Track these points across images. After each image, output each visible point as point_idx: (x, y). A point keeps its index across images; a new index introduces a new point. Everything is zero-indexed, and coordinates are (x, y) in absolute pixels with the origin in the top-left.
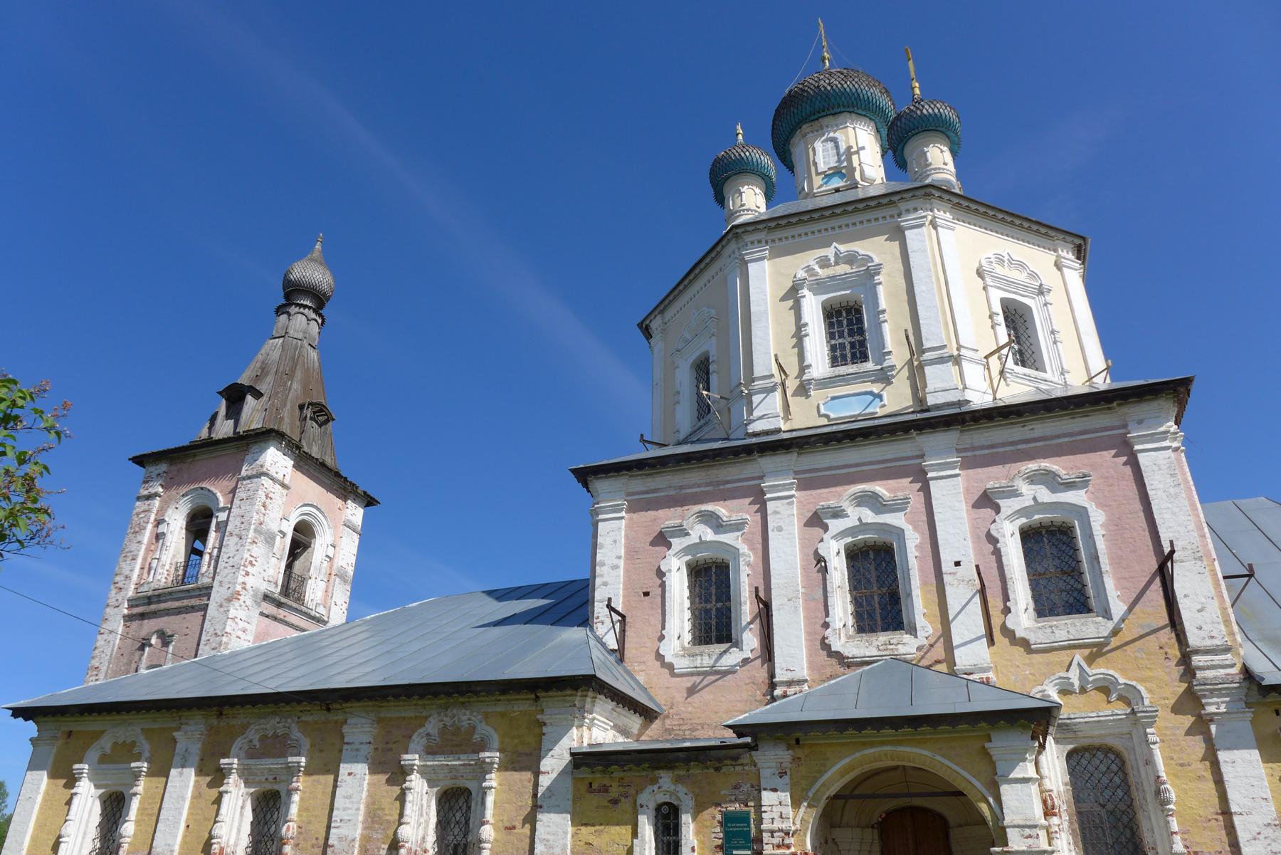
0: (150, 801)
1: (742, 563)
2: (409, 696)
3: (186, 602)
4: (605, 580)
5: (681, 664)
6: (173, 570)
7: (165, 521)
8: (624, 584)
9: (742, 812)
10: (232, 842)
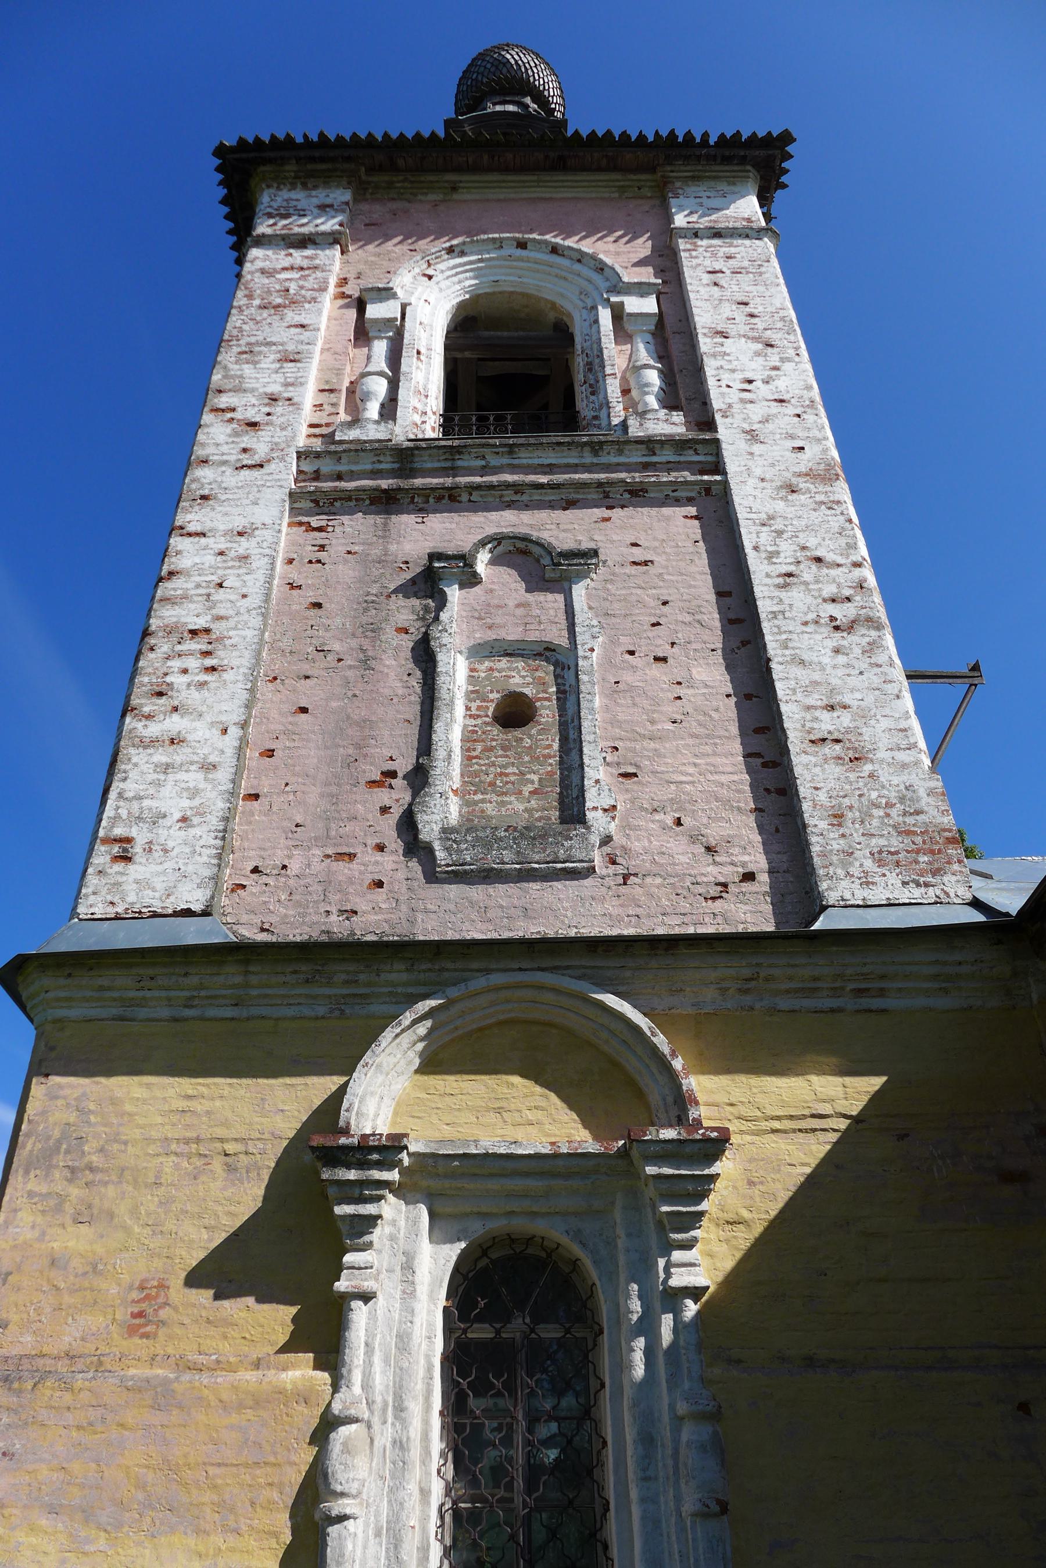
7: (394, 296)
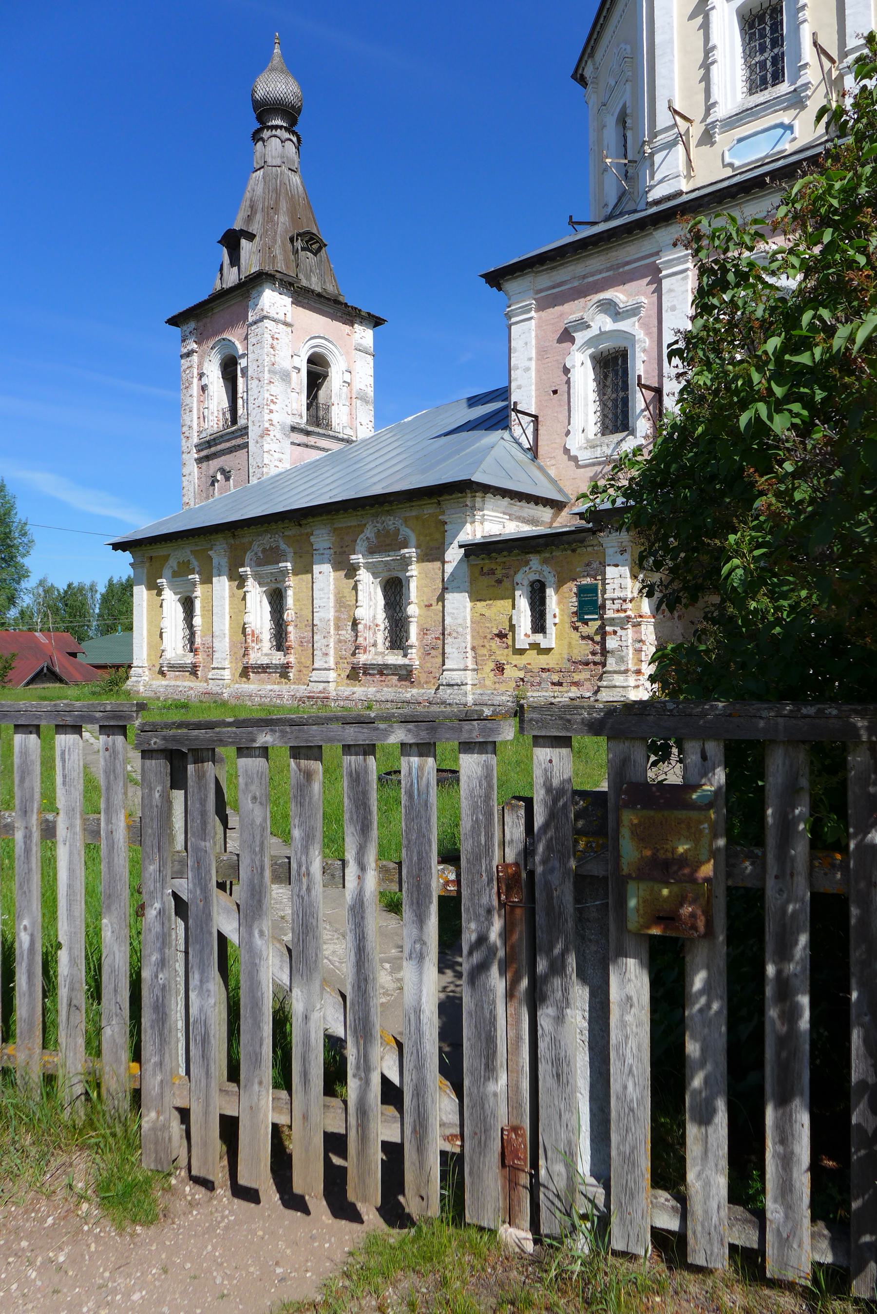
1: (637, 350)
2: (363, 507)
3: (234, 442)
4: (518, 383)
5: (584, 456)
6: (221, 416)
8: (536, 384)
9: (591, 585)
10: (258, 626)
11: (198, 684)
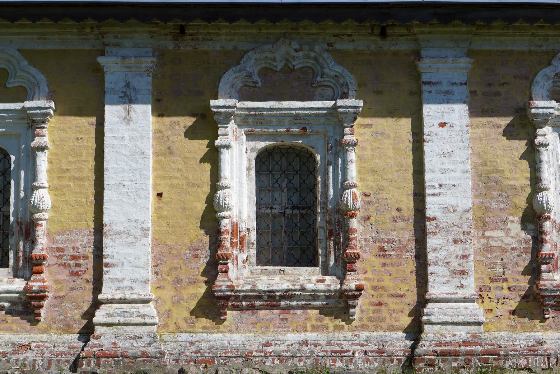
0: (70, 159)
11: (38, 337)
